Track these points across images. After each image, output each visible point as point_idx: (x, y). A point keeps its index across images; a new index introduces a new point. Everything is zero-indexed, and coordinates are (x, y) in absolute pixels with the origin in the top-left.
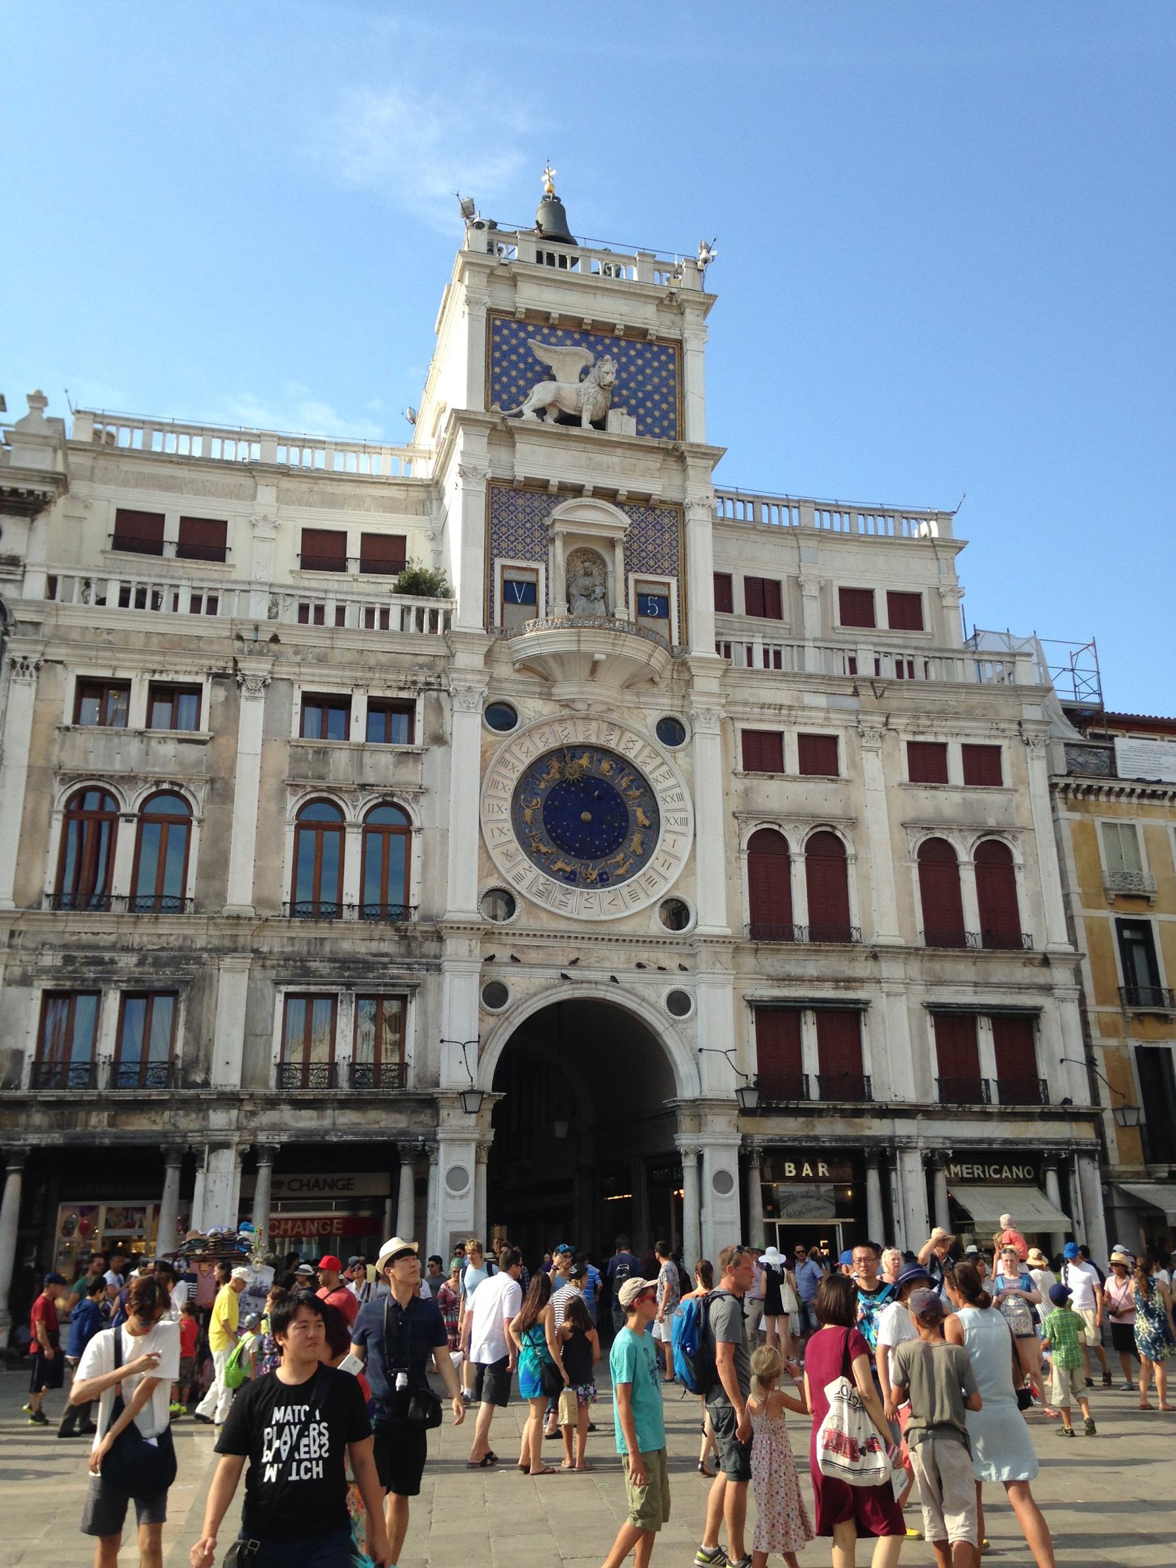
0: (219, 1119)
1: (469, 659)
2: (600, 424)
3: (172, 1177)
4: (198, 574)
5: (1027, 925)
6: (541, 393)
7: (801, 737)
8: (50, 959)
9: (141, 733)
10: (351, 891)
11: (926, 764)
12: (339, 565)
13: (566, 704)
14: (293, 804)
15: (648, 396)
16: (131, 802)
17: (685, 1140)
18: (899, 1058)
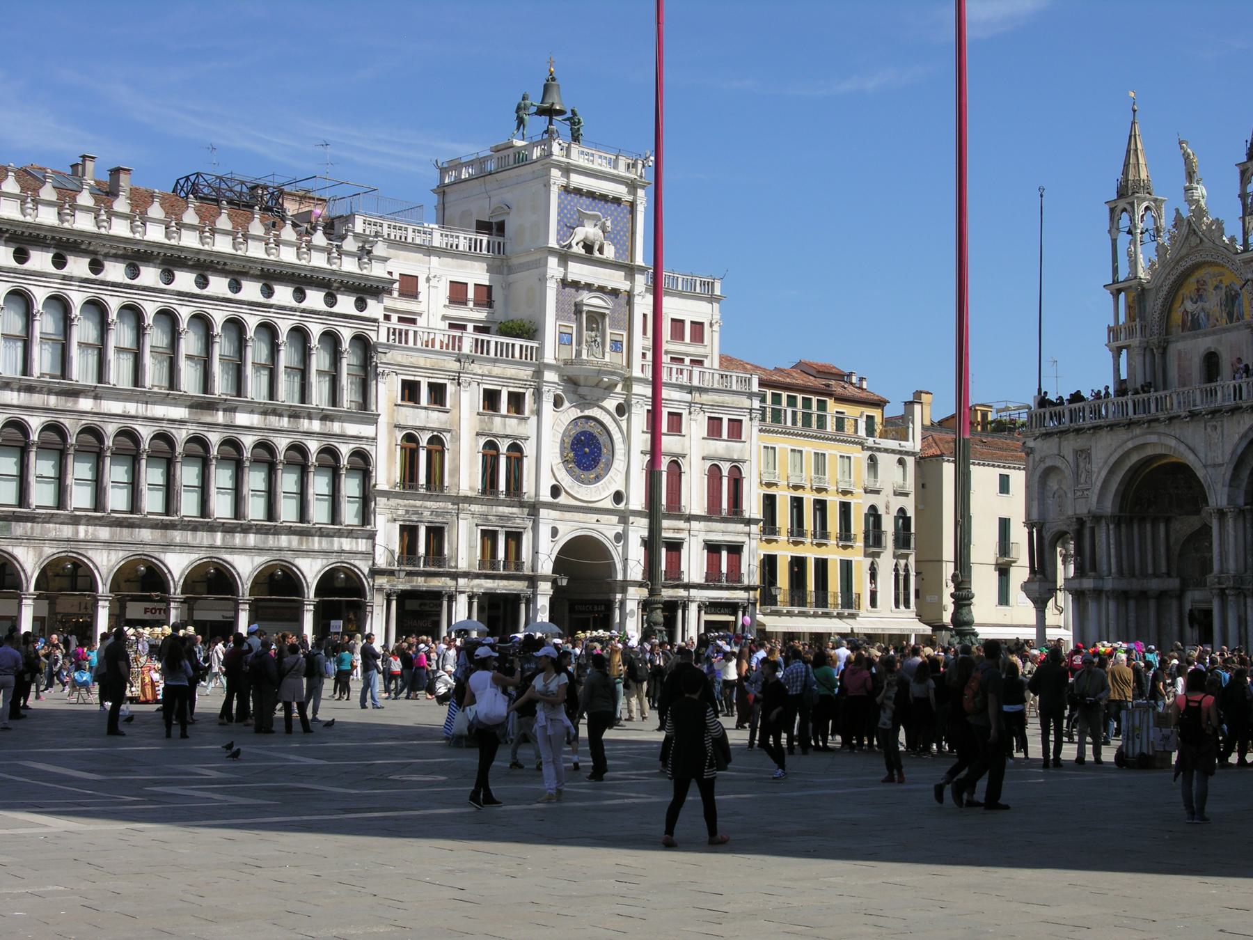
0: (462, 581)
1: (550, 376)
2: (601, 250)
3: (445, 604)
4: (406, 305)
5: (745, 506)
6: (581, 233)
7: (669, 413)
8: (401, 512)
9: (425, 408)
10: (502, 486)
11: (714, 428)
12: (464, 302)
13: (583, 397)
14: (482, 441)
15: (619, 232)
16: (424, 439)
17: (619, 596)
18: (694, 565)
